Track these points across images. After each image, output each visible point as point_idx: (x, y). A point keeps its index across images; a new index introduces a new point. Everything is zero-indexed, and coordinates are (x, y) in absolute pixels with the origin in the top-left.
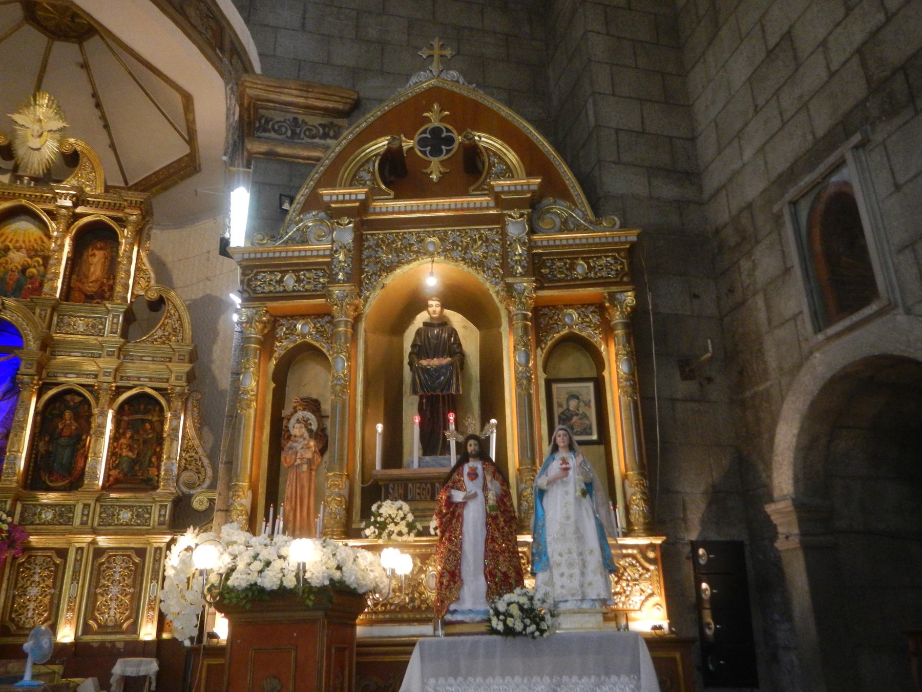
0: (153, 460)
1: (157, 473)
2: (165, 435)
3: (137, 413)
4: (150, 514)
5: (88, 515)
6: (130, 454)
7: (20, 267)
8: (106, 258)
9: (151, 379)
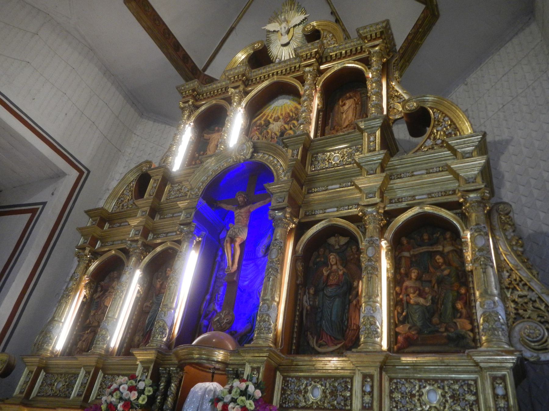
0: (459, 306)
1: (469, 327)
2: (469, 267)
3: (420, 246)
4: (476, 394)
5: (371, 393)
6: (421, 301)
7: (278, 134)
8: (357, 104)
9: (430, 195)
